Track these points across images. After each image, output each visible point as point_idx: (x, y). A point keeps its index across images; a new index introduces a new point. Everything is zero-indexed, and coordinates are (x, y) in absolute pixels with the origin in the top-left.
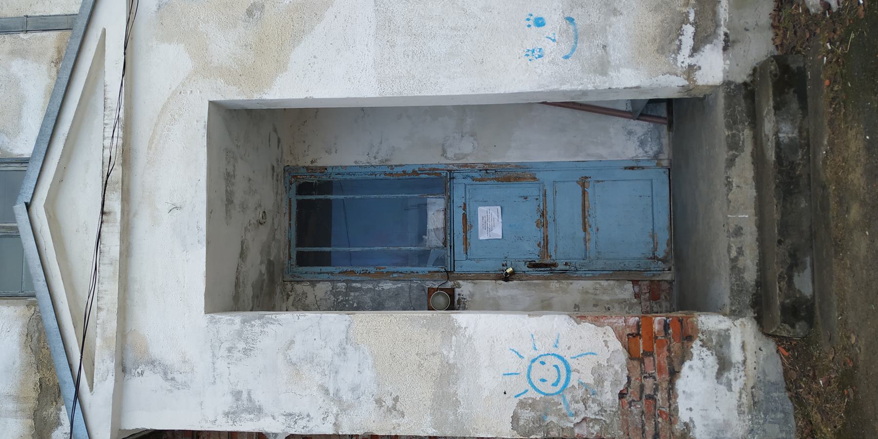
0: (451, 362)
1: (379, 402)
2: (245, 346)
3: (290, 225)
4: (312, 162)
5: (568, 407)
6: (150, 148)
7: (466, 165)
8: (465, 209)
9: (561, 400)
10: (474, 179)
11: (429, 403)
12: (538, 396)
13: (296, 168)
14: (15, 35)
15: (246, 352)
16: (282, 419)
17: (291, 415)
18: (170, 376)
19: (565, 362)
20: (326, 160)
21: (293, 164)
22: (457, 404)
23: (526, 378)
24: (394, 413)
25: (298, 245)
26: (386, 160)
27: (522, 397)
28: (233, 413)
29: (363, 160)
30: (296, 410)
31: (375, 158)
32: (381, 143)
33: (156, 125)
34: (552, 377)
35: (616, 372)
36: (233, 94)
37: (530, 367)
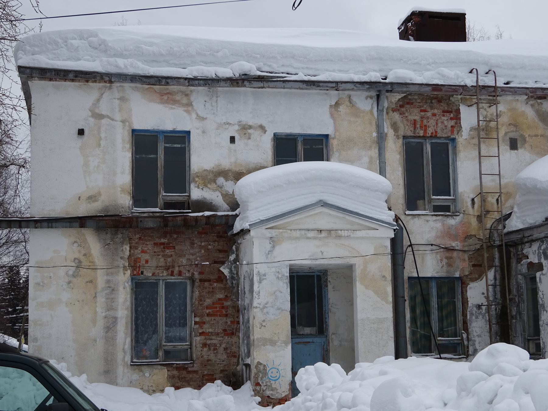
0: (277, 344)
1: (264, 321)
2: (280, 277)
3: (305, 273)
4: (329, 281)
5: (264, 380)
6: (341, 244)
7: (329, 343)
8: (312, 342)
9: (266, 378)
10: (324, 346)
11: (264, 336)
12: (267, 371)
13: (327, 275)
14: (378, 158)
15: (278, 278)
16: (258, 290)
17: (259, 293)
18: (270, 253)
19: (278, 379)
20: (330, 287)
21: (329, 274)
22: (264, 346)
23: (272, 367)
24: (261, 326)
25: (297, 276)
26: (330, 311)
27: (267, 366)
28: (259, 274)
29: (331, 301)
30: (260, 294)
31: (331, 306)
32: (337, 309)
33: (348, 246)
34: (273, 375)
35: (275, 395)
36: (358, 272)
37: (276, 368)
